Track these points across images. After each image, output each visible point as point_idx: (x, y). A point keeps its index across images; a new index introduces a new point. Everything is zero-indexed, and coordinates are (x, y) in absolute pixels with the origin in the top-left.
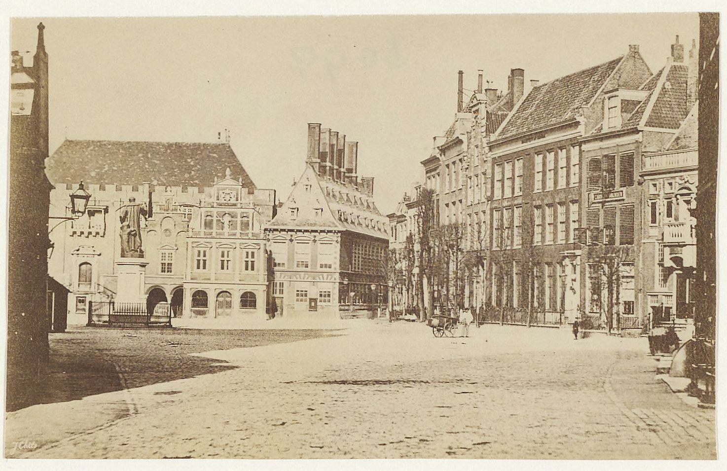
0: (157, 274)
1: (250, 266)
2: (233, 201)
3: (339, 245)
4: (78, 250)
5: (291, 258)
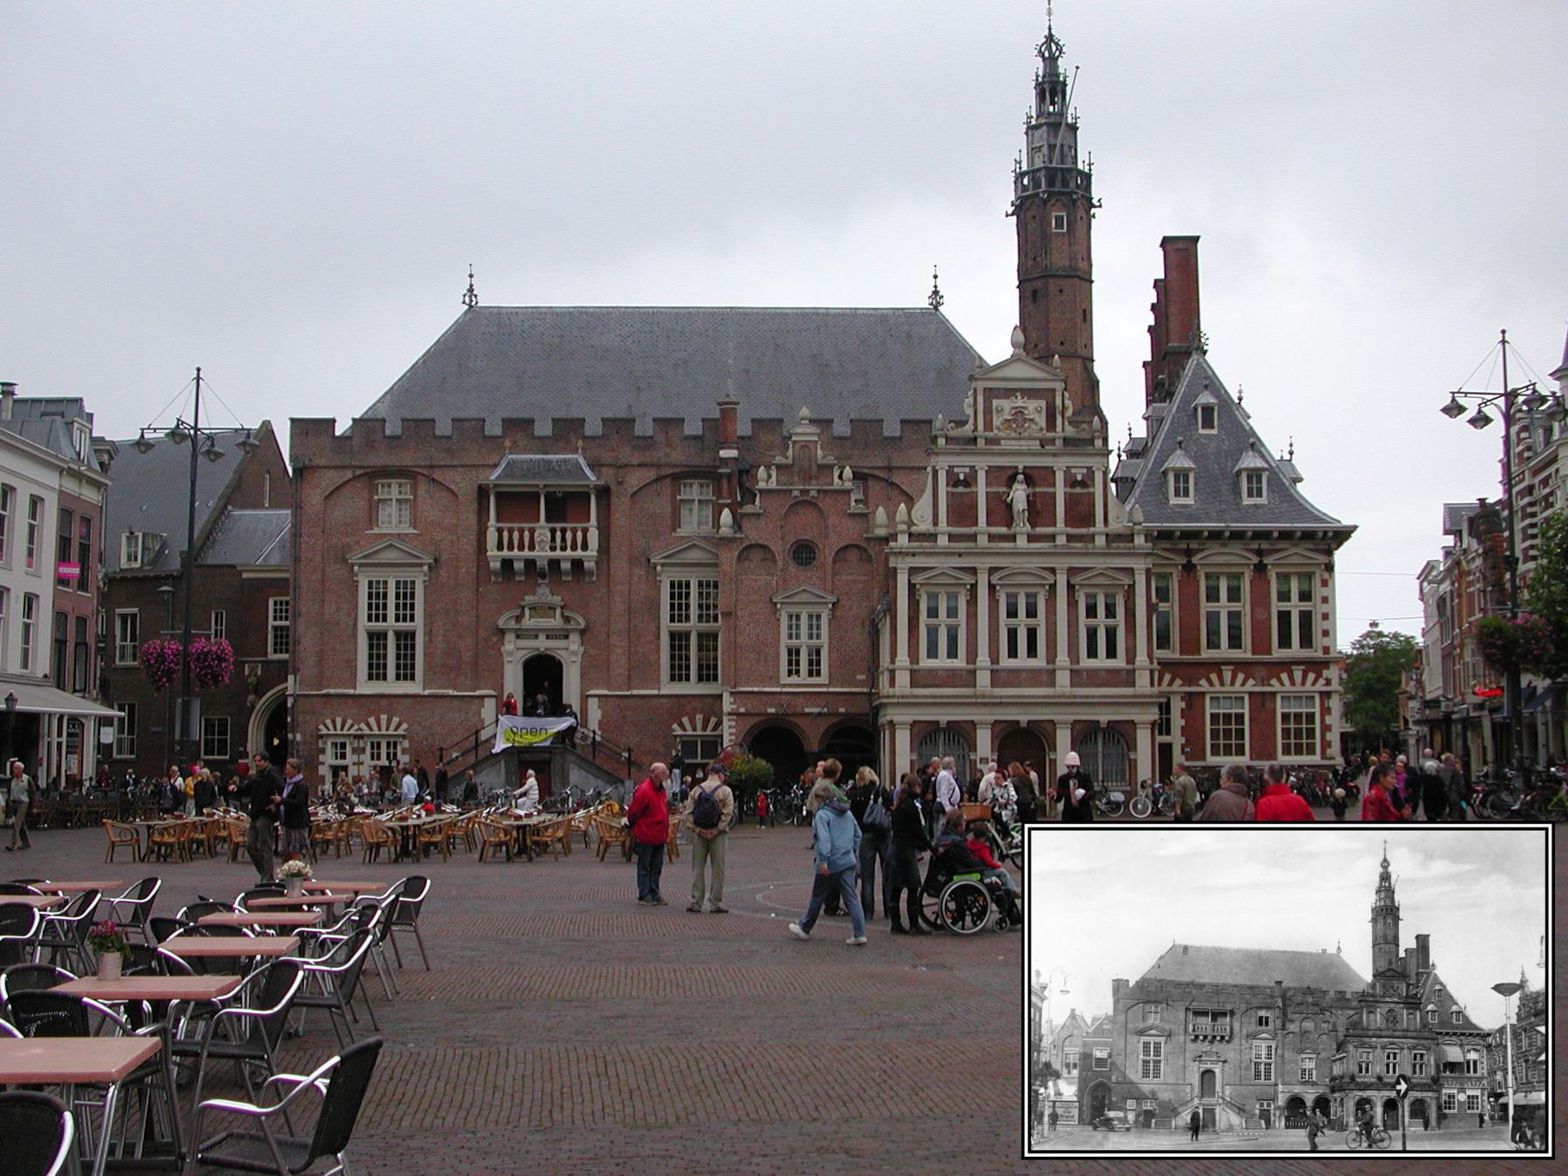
0: (778, 684)
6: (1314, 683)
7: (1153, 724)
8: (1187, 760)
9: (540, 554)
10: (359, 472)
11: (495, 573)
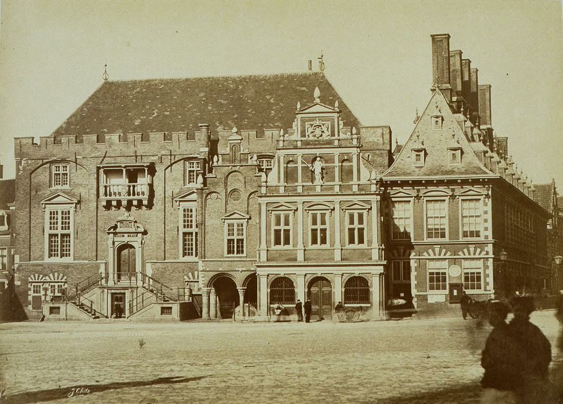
0: (223, 257)
1: (356, 236)
2: (325, 137)
3: (489, 202)
4: (115, 227)
5: (418, 226)
6: (479, 254)
7: (380, 274)
8: (418, 291)
9: (123, 197)
10: (45, 161)
11: (103, 206)
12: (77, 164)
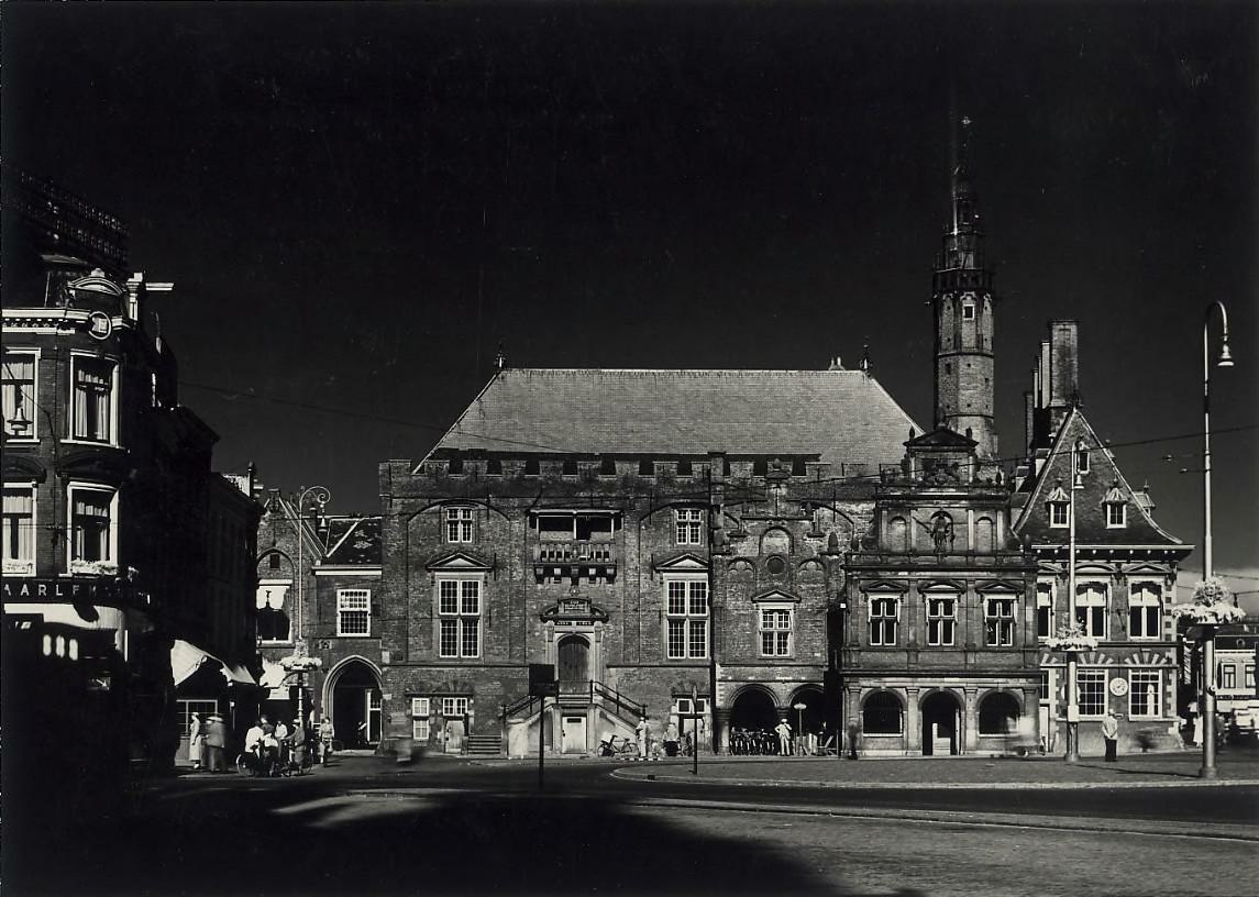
12: (489, 506)
